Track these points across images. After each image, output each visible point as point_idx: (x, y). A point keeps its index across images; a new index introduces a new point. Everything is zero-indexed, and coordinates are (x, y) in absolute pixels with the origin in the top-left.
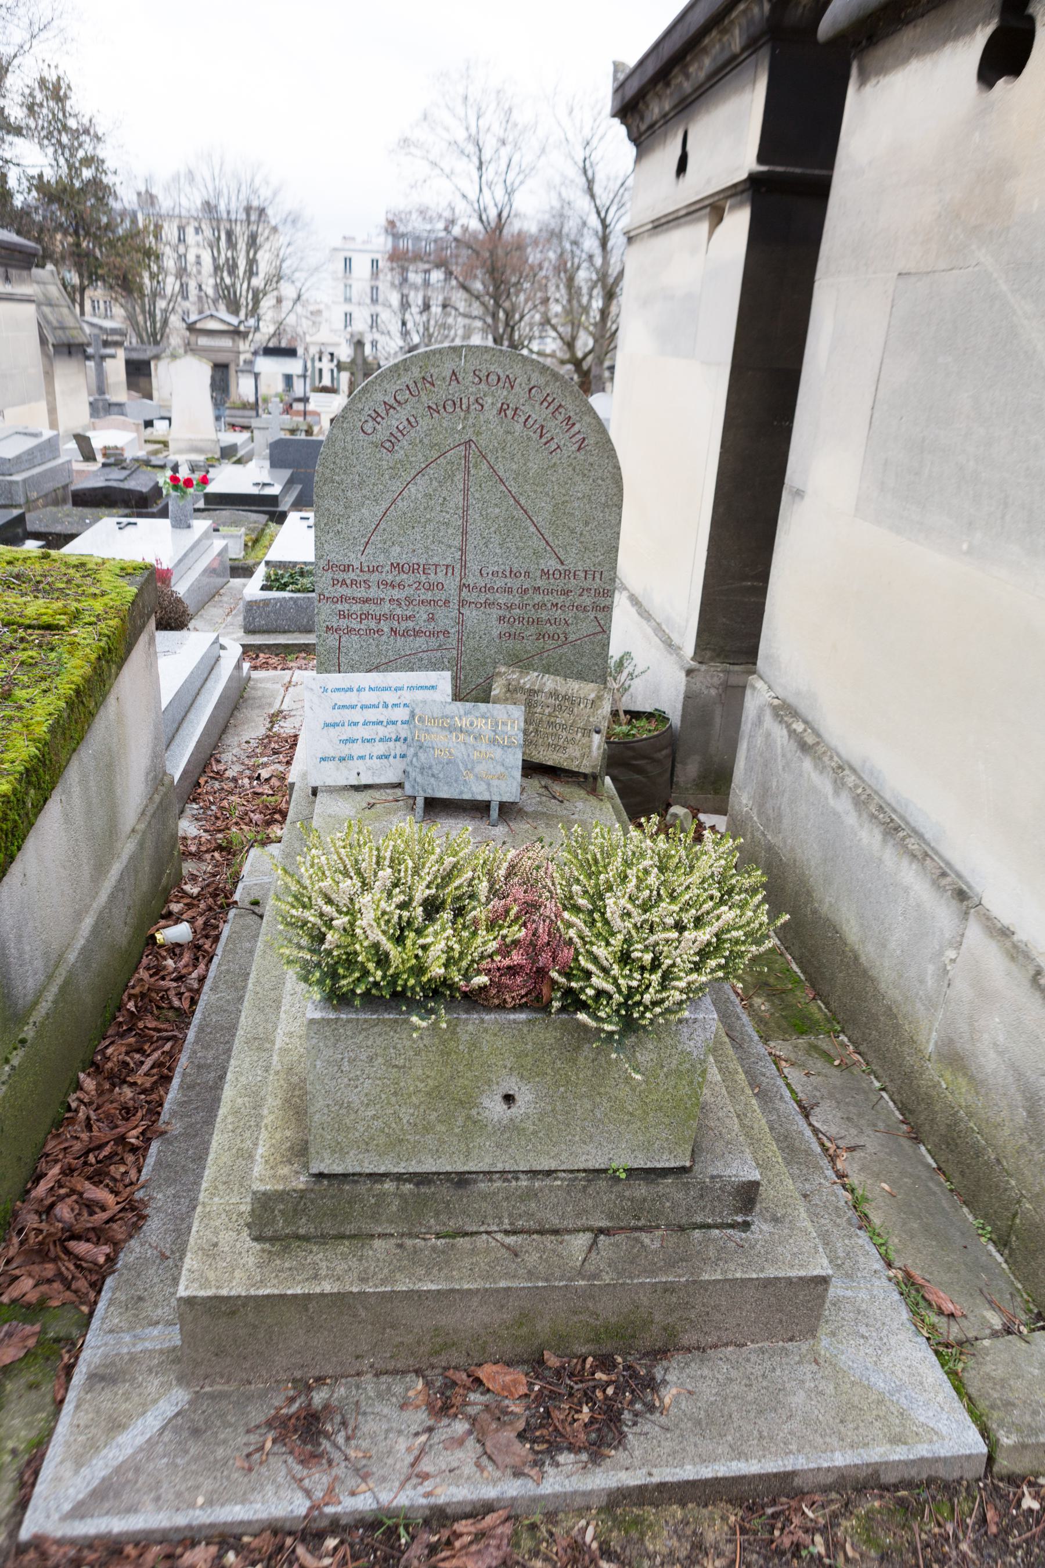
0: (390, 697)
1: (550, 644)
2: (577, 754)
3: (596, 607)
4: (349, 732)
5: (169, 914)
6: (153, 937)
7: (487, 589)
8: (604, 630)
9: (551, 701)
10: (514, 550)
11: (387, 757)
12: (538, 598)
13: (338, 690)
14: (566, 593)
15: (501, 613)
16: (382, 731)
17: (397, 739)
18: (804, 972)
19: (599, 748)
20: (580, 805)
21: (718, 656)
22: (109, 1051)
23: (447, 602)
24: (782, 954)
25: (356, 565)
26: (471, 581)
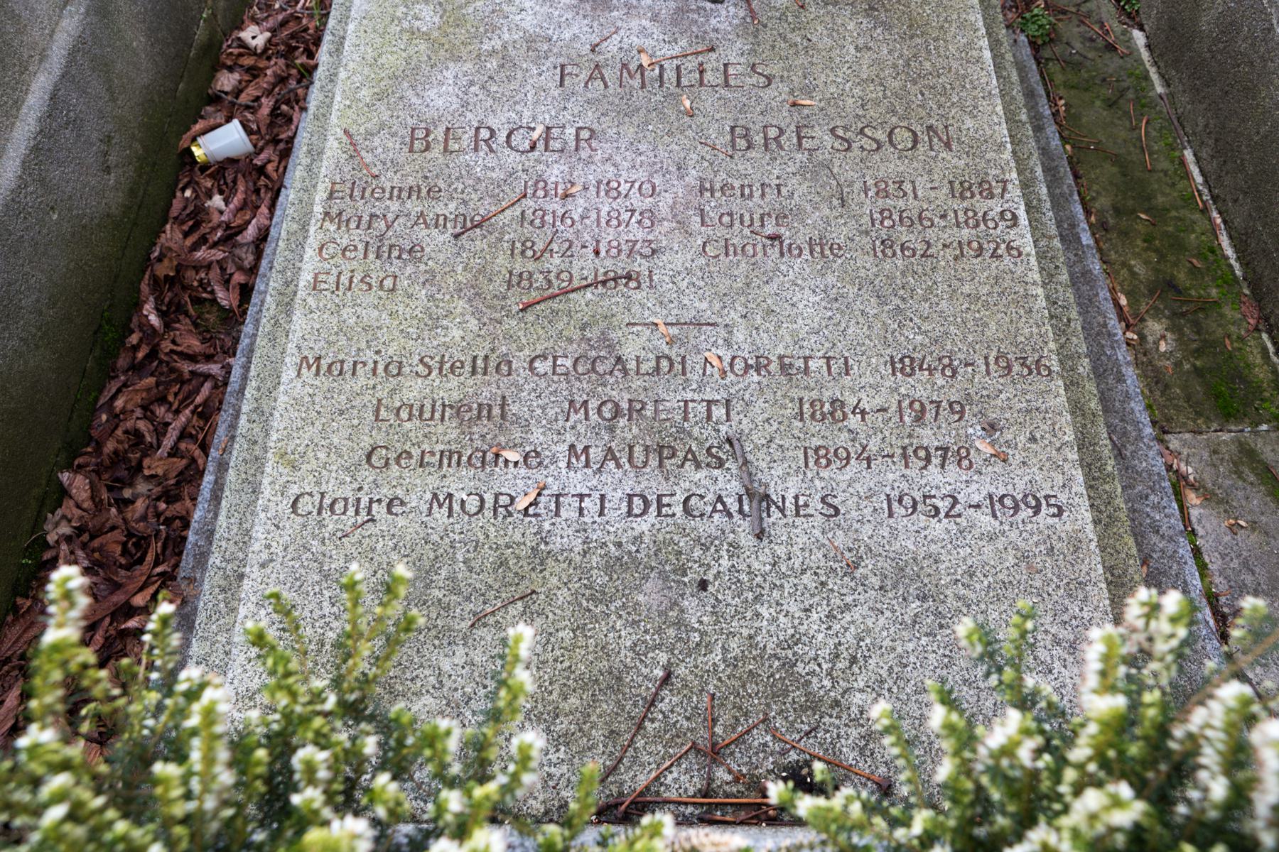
5: (216, 99)
18: (1245, 264)
22: (119, 403)
24: (1205, 211)
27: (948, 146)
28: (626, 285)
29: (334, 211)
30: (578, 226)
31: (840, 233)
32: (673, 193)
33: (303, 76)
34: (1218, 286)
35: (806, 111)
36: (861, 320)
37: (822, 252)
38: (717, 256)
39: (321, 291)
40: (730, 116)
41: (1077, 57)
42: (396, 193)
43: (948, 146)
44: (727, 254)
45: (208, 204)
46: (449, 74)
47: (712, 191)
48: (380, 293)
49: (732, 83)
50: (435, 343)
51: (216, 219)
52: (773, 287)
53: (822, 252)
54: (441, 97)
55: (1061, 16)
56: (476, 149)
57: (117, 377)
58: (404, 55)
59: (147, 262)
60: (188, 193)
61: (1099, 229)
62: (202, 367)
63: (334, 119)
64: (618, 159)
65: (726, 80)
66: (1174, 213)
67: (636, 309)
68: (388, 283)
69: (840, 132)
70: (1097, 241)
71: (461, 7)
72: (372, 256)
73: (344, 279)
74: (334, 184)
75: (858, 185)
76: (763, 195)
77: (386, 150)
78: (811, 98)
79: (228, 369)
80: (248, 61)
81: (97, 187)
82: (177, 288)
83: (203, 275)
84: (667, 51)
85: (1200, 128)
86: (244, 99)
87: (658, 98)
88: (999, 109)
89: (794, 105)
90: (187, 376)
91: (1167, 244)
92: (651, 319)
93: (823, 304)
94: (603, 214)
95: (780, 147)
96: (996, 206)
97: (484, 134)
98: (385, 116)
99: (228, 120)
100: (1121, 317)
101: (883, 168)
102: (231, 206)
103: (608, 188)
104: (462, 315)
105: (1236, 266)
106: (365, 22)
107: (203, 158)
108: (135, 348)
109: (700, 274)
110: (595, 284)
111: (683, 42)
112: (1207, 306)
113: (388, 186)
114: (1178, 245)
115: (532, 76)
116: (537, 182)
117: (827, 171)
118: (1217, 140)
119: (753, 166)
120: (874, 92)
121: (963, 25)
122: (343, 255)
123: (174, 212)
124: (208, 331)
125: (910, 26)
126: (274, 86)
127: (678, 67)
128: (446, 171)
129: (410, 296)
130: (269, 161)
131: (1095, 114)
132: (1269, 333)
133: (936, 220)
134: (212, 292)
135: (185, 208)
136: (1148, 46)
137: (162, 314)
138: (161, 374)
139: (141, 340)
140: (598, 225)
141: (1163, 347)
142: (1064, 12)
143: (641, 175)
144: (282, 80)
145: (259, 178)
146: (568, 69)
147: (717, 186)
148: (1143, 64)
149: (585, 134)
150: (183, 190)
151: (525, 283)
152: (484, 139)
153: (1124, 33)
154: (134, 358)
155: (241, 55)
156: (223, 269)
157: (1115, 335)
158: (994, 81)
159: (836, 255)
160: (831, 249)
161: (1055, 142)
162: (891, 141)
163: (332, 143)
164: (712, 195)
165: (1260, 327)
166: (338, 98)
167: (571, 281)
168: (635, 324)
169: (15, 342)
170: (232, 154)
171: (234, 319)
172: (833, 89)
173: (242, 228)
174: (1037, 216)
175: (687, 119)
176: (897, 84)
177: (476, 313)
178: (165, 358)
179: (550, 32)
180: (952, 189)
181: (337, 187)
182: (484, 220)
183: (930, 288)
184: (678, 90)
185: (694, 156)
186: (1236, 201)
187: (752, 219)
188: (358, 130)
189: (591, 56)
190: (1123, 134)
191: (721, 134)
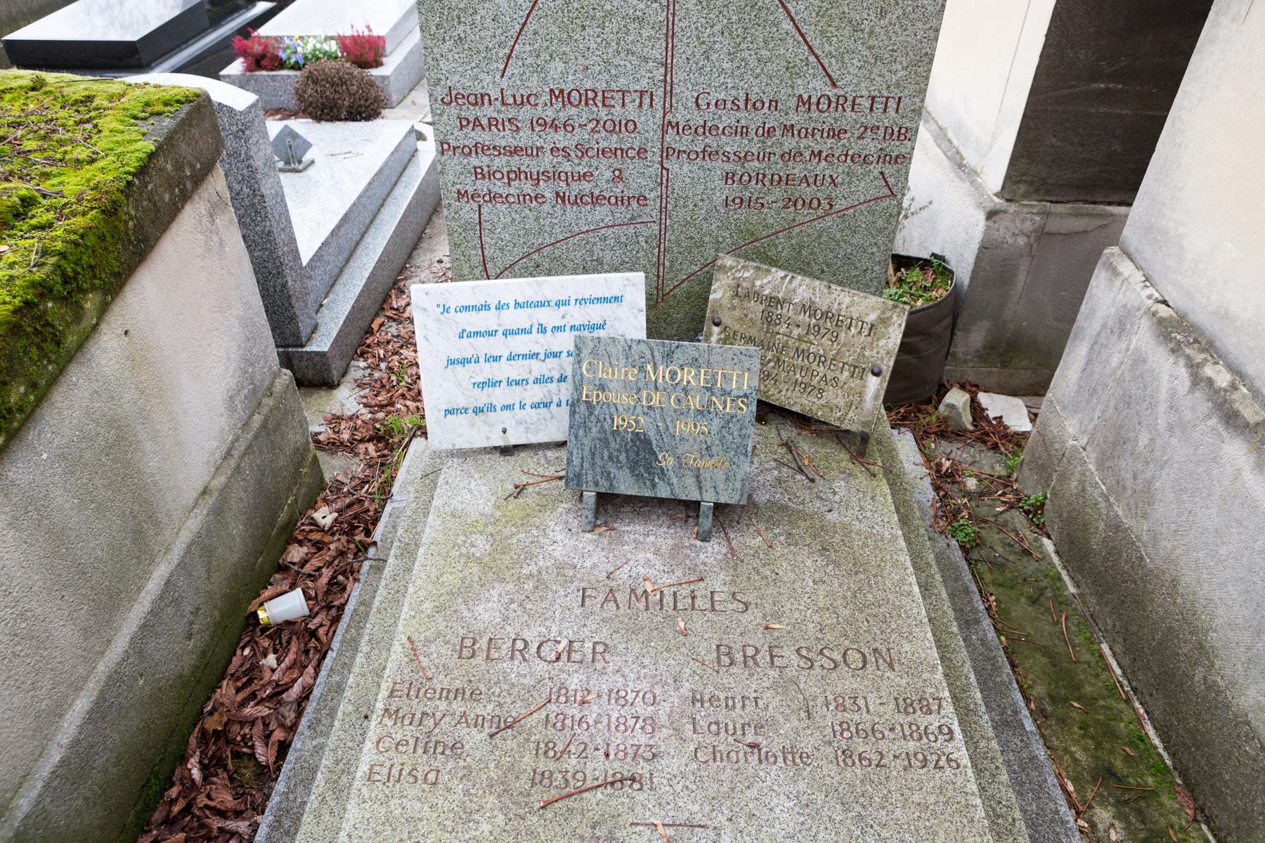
0: (549, 317)
1: (805, 214)
2: (841, 402)
3: (884, 157)
4: (486, 371)
5: (283, 569)
6: (255, 614)
7: (707, 129)
8: (894, 191)
9: (802, 318)
10: (753, 63)
11: (546, 405)
12: (789, 143)
13: (466, 308)
14: (836, 134)
15: (729, 167)
16: (538, 368)
17: (562, 379)
18: (1173, 755)
19: (876, 397)
20: (839, 485)
21: (1037, 191)
23: (642, 152)
24: (1128, 701)
25: (495, 94)
26: (680, 116)
27: (891, 666)
28: (631, 786)
29: (393, 708)
30: (592, 730)
31: (808, 743)
32: (672, 702)
33: (359, 550)
34: (1152, 775)
35: (776, 634)
36: (829, 826)
37: (794, 760)
38: (706, 762)
39: (374, 782)
40: (716, 636)
42: (445, 694)
43: (891, 666)
44: (715, 760)
45: (263, 662)
47: (702, 702)
48: (424, 786)
49: (717, 608)
50: (467, 836)
51: (267, 676)
52: (753, 792)
53: (794, 760)
54: (487, 612)
56: (512, 658)
57: (150, 831)
59: (200, 715)
60: (247, 652)
61: (1039, 715)
62: (231, 825)
63: (400, 628)
64: (626, 671)
65: (713, 606)
66: (1102, 703)
67: (638, 809)
68: (432, 777)
69: (804, 652)
70: (1039, 727)
71: (507, 538)
72: (420, 751)
73: (395, 772)
74: (395, 683)
75: (820, 700)
76: (744, 706)
77: (440, 655)
78: (780, 622)
79: (255, 827)
80: (316, 536)
81: (178, 653)
82: (222, 742)
83: (247, 731)
84: (666, 580)
85: (1109, 627)
86: (308, 569)
87: (659, 619)
88: (930, 635)
89: (767, 628)
90: (215, 833)
91: (1102, 733)
92: (651, 820)
93: (797, 809)
94: (613, 719)
95: (756, 664)
96: (934, 721)
97: (520, 645)
98: (442, 626)
99: (293, 587)
100: (1072, 805)
101: (840, 685)
102: (283, 665)
103: (617, 696)
104: (492, 810)
105: (1165, 755)
107: (266, 620)
108: (173, 802)
109: (692, 778)
110: (605, 785)
112: (1146, 795)
113: (438, 687)
114: (1112, 735)
116: (560, 689)
117: (795, 687)
118: (1125, 640)
119: (735, 681)
120: (830, 619)
121: (895, 564)
122: (397, 749)
123: (232, 669)
124: (242, 786)
125: (855, 564)
126: (335, 558)
127: (675, 593)
128: (487, 676)
129: (449, 790)
130: (322, 625)
131: (1021, 609)
132: (1208, 824)
133: (887, 733)
134: (252, 747)
135: (242, 665)
136: (1057, 552)
137: (203, 767)
138: (191, 829)
139: (179, 794)
140: (609, 730)
141: (1114, 837)
142: (986, 522)
143: (644, 686)
144: (342, 554)
145: (307, 640)
146: (588, 592)
147: (706, 698)
148: (1054, 567)
149: (600, 648)
150: (243, 649)
151: (546, 782)
152: (519, 650)
153: (1036, 540)
154: (170, 811)
155: (311, 531)
156: (266, 725)
157: (1068, 822)
159: (805, 764)
160: (801, 757)
161: (991, 634)
162: (845, 661)
163: (397, 648)
164: (702, 706)
165: (1199, 818)
167: (584, 780)
168: (637, 824)
169: (80, 802)
170: (290, 617)
171: (268, 774)
172: (797, 615)
173: (288, 687)
174: (976, 719)
176: (847, 612)
177: (504, 809)
178: (197, 812)
180: (898, 705)
181: (397, 687)
182: (515, 722)
183: (885, 796)
184: (675, 613)
185: (687, 670)
186: (1151, 695)
187: (735, 728)
188: (419, 638)
190: (1048, 628)
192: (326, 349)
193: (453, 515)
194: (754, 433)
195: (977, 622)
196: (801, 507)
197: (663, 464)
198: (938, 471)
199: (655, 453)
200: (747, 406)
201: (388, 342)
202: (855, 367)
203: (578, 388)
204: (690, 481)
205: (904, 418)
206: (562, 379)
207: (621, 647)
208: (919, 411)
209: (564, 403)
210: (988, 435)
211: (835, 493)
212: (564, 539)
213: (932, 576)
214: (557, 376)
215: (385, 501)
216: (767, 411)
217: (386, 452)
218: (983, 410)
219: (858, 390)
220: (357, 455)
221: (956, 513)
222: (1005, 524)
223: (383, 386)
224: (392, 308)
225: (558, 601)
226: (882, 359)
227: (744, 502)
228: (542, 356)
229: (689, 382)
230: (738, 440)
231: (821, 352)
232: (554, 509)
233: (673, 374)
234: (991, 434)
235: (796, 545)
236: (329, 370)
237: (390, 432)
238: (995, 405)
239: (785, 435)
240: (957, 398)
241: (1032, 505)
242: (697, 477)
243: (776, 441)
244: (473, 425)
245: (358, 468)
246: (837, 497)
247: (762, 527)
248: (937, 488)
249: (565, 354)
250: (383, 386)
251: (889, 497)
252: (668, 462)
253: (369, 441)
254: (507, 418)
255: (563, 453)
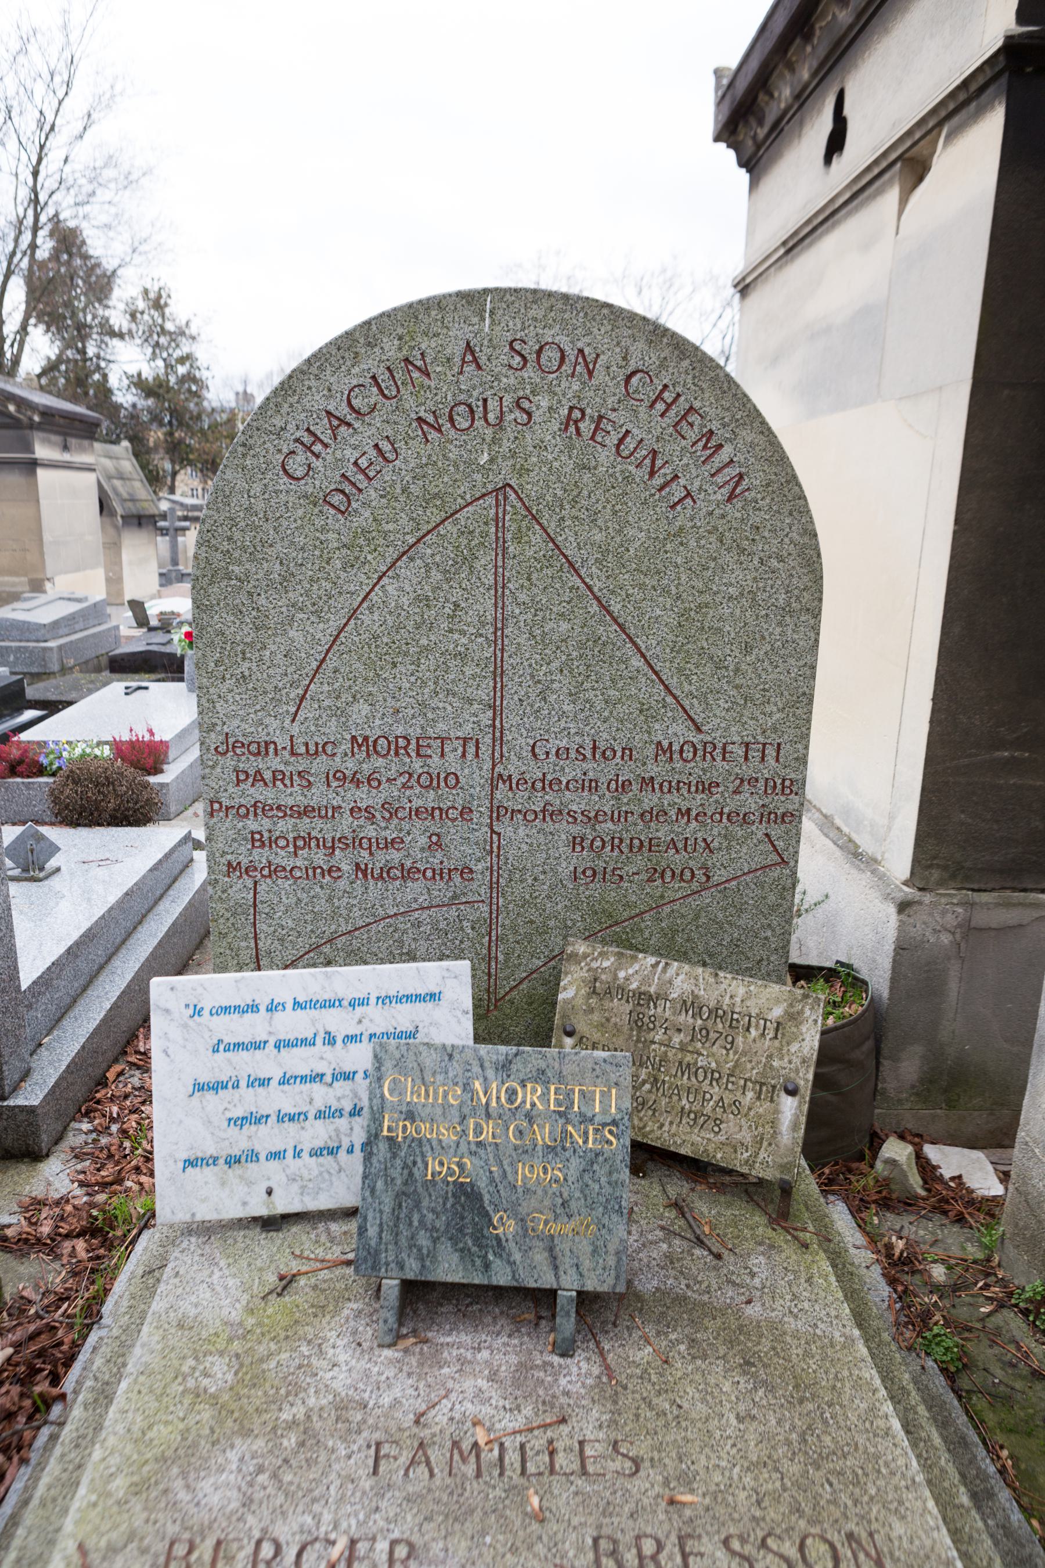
0: (339, 1021)
1: (676, 889)
2: (746, 1136)
3: (767, 815)
4: (248, 1100)
7: (547, 784)
8: (785, 860)
9: (685, 1019)
10: (599, 705)
11: (332, 1152)
12: (650, 800)
13: (226, 1010)
14: (707, 788)
15: (576, 830)
16: (321, 1095)
17: (356, 1112)
19: (795, 1127)
20: (758, 1261)
21: (953, 877)
23: (466, 811)
25: (282, 741)
26: (513, 768)
33: (37, 1410)
35: (688, 1512)
41: (1002, 1388)
46: (233, 1456)
49: (591, 1469)
55: (966, 1335)
58: (181, 1426)
65: (583, 1466)
71: (261, 1360)
78: (692, 1491)
84: (509, 1422)
87: (499, 1492)
88: (931, 1504)
89: (672, 1502)
106: (142, 1378)
111: (528, 1411)
115: (338, 1459)
121: (858, 1384)
125: (797, 1386)
127: (522, 1446)
142: (970, 1330)
158: (914, 1463)
161: (1016, 1516)
166: (82, 1491)
172: (717, 1477)
175: (535, 1526)
176: (795, 1469)
179: (366, 1395)
184: (523, 1481)
188: (97, 1543)
189: (415, 1430)
191: (580, 1549)
192: (36, 1103)
193: (180, 1326)
194: (629, 1189)
195: (991, 1495)
196: (706, 1298)
197: (500, 1231)
198: (889, 1255)
199: (487, 1215)
200: (617, 1137)
201: (126, 1097)
202: (762, 1084)
203: (376, 1119)
204: (540, 1257)
205: (830, 1182)
206: (356, 1112)
207: (437, 1547)
208: (850, 1171)
209: (357, 1148)
210: (947, 1202)
211: (753, 1275)
212: (348, 1361)
213: (913, 1408)
214: (348, 1107)
215: (89, 1327)
216: (647, 1157)
217: (102, 1251)
218: (935, 1168)
219: (770, 1118)
220: (58, 1257)
221: (926, 1316)
222: (998, 1332)
223: (110, 1156)
224: (138, 1052)
225: (336, 1467)
226: (797, 1071)
227: (621, 1288)
228: (328, 1079)
229: (533, 1105)
230: (607, 1190)
231: (713, 1065)
232: (336, 1312)
233: (512, 1094)
234: (951, 1202)
235: (704, 1357)
236: (36, 1134)
237: (111, 1222)
238: (950, 1161)
239: (672, 1192)
240: (896, 1150)
241: (1029, 1300)
242: (551, 1250)
243: (661, 1200)
244: (223, 1184)
245: (56, 1277)
246: (757, 1281)
247: (650, 1330)
248: (892, 1282)
249: (360, 1075)
250: (110, 1156)
251: (833, 1279)
252: (506, 1227)
253: (78, 1236)
254: (273, 1173)
255: (353, 1226)
